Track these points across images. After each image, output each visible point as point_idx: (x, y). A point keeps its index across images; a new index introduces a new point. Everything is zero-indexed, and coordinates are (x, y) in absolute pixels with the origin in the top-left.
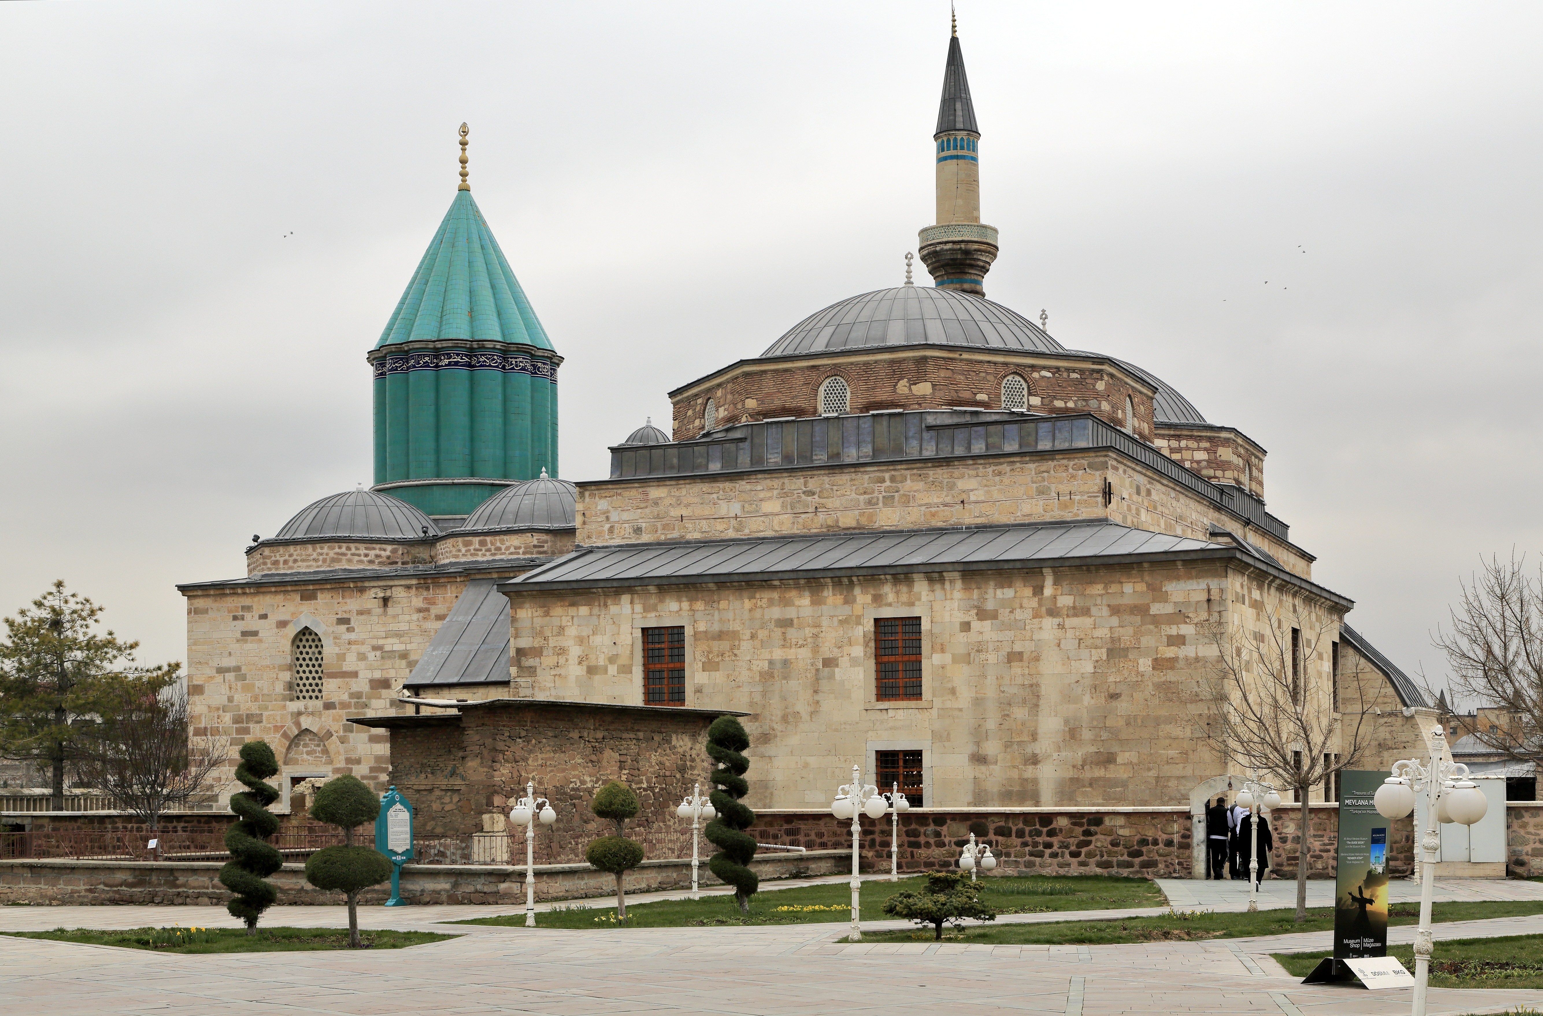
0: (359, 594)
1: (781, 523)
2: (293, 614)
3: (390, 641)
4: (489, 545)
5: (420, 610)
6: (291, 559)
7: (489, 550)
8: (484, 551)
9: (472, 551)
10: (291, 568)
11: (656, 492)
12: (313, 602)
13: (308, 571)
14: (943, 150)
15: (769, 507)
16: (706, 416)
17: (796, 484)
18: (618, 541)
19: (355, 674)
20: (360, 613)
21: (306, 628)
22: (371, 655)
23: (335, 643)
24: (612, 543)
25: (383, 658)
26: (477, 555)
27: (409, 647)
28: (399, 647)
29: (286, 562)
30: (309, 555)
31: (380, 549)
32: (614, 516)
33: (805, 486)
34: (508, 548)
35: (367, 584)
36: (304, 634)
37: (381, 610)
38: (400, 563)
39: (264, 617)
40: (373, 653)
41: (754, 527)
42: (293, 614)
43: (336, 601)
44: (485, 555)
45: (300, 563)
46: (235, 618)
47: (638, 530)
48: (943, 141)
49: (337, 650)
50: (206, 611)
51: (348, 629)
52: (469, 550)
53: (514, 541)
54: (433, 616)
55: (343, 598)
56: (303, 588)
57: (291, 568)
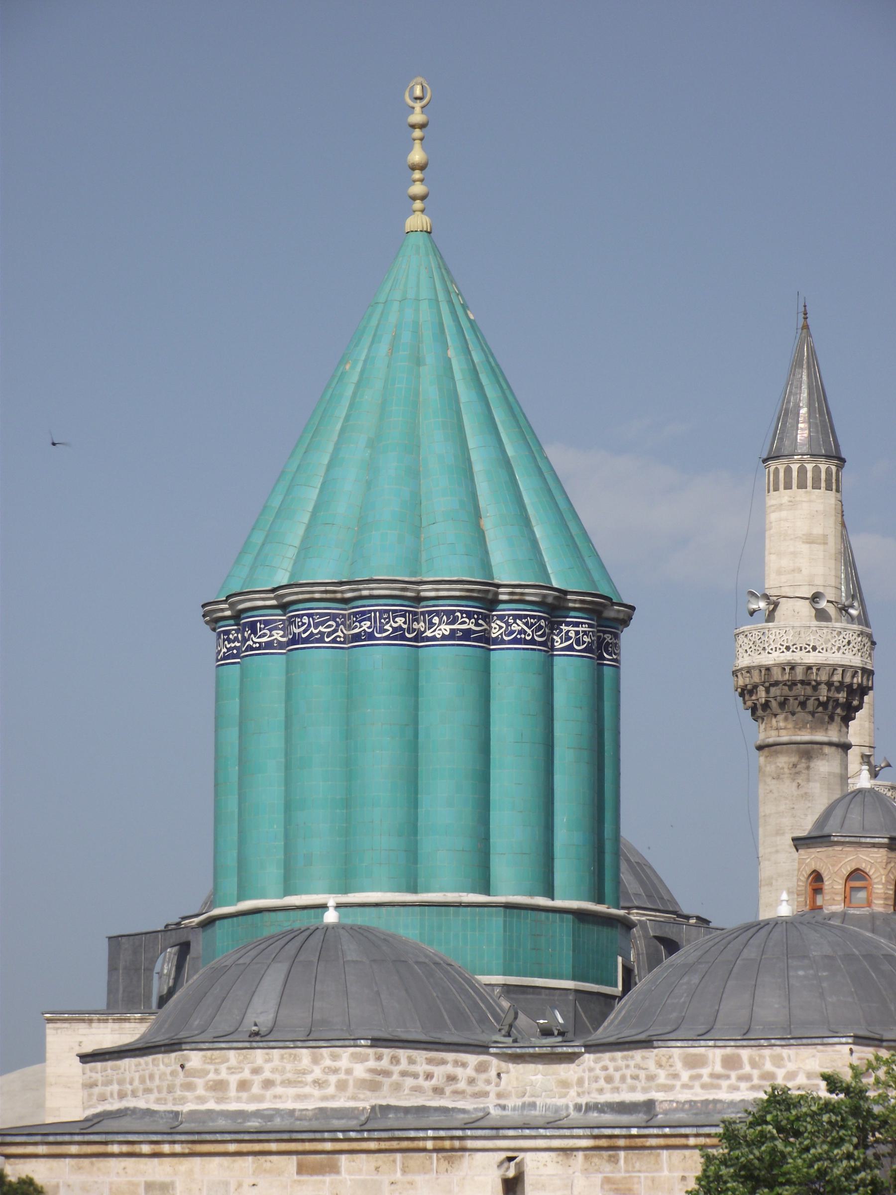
0: (444, 1164)
4: (747, 1069)
6: (258, 1079)
7: (747, 1078)
8: (733, 1080)
9: (706, 1079)
10: (260, 1099)
12: (328, 1179)
13: (298, 1106)
26: (718, 1087)
29: (243, 1085)
30: (304, 1072)
31: (456, 1063)
38: (492, 1095)
43: (385, 1179)
44: (737, 1089)
45: (279, 1090)
52: (699, 1077)
55: (404, 1171)
56: (308, 1146)
57: (260, 1099)
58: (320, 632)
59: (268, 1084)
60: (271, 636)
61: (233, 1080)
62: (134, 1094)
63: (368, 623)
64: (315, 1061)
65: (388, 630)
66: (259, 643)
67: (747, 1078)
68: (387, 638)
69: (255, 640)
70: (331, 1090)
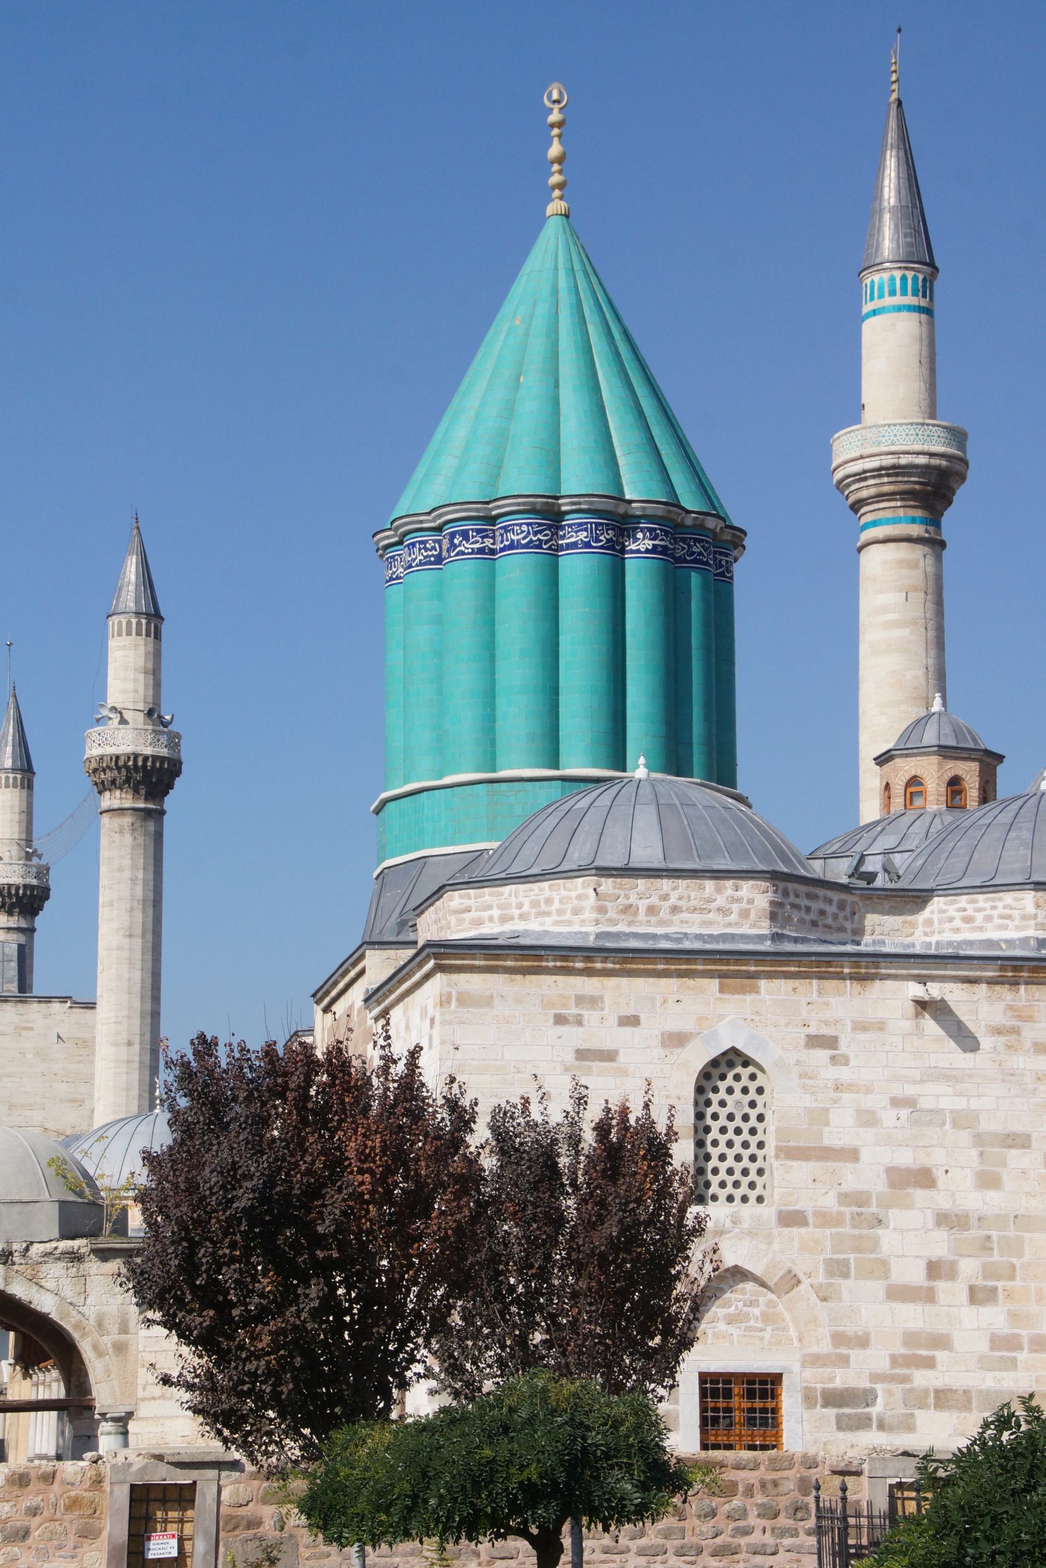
2: (701, 1019)
3: (931, 1088)
6: (666, 905)
12: (749, 998)
14: (892, 293)
19: (852, 1155)
20: (861, 1027)
21: (734, 1050)
22: (889, 1117)
23: (804, 1086)
27: (975, 1104)
28: (949, 1103)
29: (652, 910)
36: (731, 1065)
37: (908, 1025)
39: (631, 1021)
40: (893, 1113)
42: (701, 1019)
45: (685, 916)
46: (560, 1020)
48: (892, 279)
49: (808, 1101)
50: (488, 1001)
51: (833, 1058)
54: (1028, 1044)
58: (539, 540)
59: (675, 909)
60: (483, 543)
61: (643, 905)
62: (523, 917)
63: (585, 534)
64: (719, 890)
65: (601, 541)
66: (473, 549)
68: (601, 547)
69: (467, 546)
70: (734, 917)
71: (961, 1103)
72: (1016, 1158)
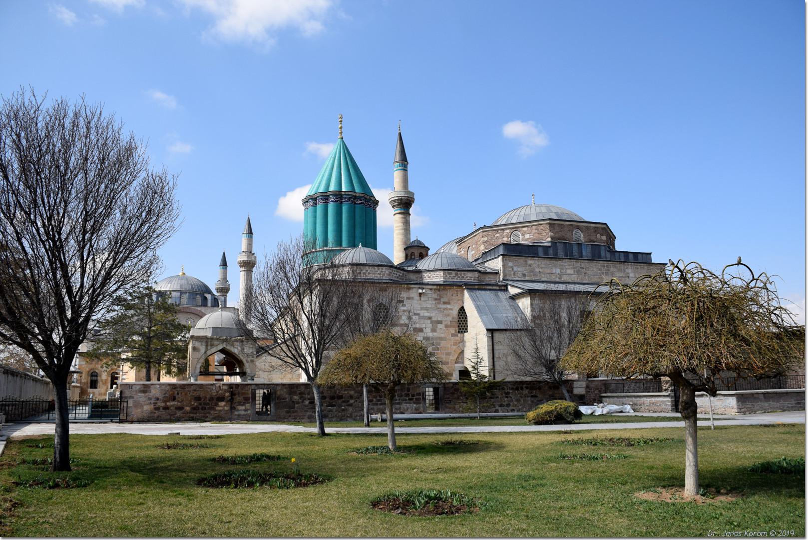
1: (574, 278)
3: (423, 311)
5: (436, 299)
7: (459, 277)
11: (530, 261)
15: (569, 271)
16: (512, 237)
17: (577, 264)
18: (517, 279)
24: (514, 279)
25: (419, 319)
27: (431, 315)
32: (515, 269)
33: (581, 265)
34: (467, 277)
35: (413, 286)
37: (419, 298)
41: (565, 279)
47: (524, 275)
53: (470, 274)
59: (369, 273)
67: (459, 277)
71: (428, 314)
72: (440, 326)
